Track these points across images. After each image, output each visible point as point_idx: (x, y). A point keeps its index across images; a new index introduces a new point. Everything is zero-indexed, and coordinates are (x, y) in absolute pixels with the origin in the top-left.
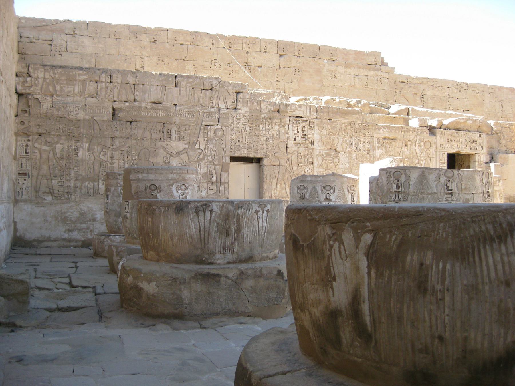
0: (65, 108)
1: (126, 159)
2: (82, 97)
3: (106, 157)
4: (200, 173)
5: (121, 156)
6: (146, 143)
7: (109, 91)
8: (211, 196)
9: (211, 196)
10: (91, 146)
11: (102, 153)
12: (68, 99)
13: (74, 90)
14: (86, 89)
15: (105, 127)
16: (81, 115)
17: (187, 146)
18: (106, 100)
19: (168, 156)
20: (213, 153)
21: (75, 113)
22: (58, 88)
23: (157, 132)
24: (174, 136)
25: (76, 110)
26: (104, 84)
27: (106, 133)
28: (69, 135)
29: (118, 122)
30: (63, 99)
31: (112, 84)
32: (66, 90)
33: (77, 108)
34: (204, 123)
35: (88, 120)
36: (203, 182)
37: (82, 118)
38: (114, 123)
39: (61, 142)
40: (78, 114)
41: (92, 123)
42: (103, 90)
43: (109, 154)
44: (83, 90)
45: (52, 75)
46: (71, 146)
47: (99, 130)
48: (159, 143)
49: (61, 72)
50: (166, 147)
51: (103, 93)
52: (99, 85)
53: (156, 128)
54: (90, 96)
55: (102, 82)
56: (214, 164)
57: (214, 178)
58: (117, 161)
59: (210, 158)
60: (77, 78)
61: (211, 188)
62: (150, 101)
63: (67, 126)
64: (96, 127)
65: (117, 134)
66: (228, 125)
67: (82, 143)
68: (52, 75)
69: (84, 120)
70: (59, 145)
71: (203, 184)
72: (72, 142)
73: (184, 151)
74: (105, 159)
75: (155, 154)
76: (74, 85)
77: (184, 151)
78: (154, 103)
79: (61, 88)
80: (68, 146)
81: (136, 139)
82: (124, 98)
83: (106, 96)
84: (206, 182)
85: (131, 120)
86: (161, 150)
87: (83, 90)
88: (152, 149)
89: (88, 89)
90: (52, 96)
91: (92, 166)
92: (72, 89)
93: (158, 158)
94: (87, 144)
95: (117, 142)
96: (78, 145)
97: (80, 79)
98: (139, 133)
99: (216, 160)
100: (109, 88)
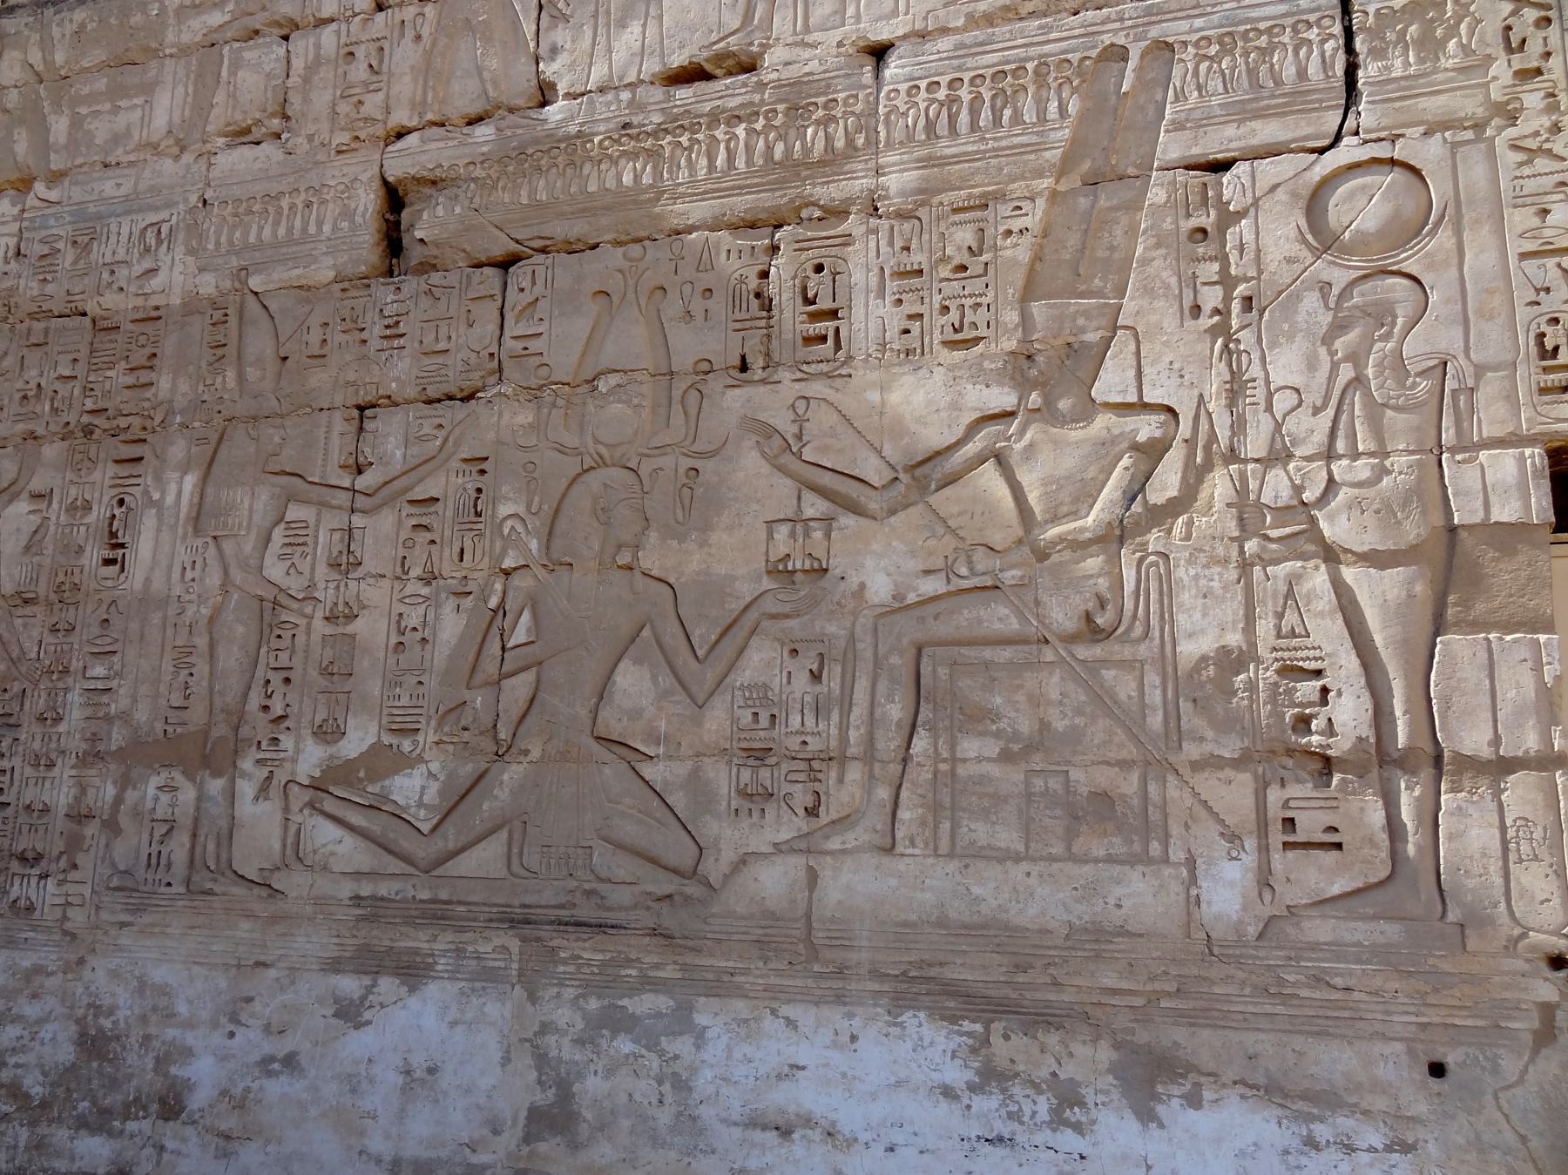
0: (87, 248)
1: (447, 566)
2: (187, 158)
3: (305, 566)
4: (1166, 660)
5: (409, 544)
6: (617, 417)
7: (359, 71)
8: (1320, 929)
9: (1320, 929)
10: (210, 491)
11: (278, 535)
12: (108, 188)
13: (145, 121)
14: (220, 97)
15: (315, 337)
16: (177, 277)
17: (1002, 398)
18: (345, 137)
19: (814, 506)
20: (1310, 429)
21: (138, 269)
22: (59, 127)
23: (718, 305)
24: (871, 317)
25: (147, 250)
26: (328, 33)
27: (319, 378)
28: (88, 431)
29: (411, 284)
30: (77, 194)
31: (380, 17)
32: (101, 130)
33: (151, 238)
34: (1170, 147)
35: (214, 305)
36: (1212, 763)
37: (176, 301)
38: (384, 293)
39: (37, 484)
40: (152, 272)
41: (222, 317)
42: (326, 73)
43: (326, 541)
44: (202, 108)
45: (35, 57)
46: (87, 507)
47: (272, 366)
48: (735, 401)
49: (83, 25)
50: (790, 430)
51: (322, 99)
52: (301, 45)
53: (708, 280)
54: (242, 135)
55: (323, 22)
56: (1331, 555)
57: (1349, 714)
58: (377, 594)
59: (1276, 487)
60: (170, 37)
61: (1310, 825)
62: (652, 66)
63: (80, 370)
64: (260, 343)
65: (400, 373)
66: (1470, 106)
67: (159, 479)
68: (35, 57)
69: (191, 307)
70: (22, 506)
71: (1209, 785)
72: (96, 476)
73: (971, 448)
74: (295, 585)
75: (695, 502)
76: (148, 89)
77: (971, 448)
78: (693, 74)
79: (76, 122)
80: (72, 509)
81: (534, 393)
82: (464, 100)
83: (344, 108)
84: (1238, 763)
85: (500, 246)
86: (750, 464)
87: (202, 108)
88: (667, 462)
89: (233, 96)
90: (24, 185)
91: (201, 642)
92: (138, 113)
93: (719, 537)
94: (190, 481)
95: (391, 440)
96: (135, 496)
97: (186, 38)
98: (563, 340)
99: (1356, 505)
100: (361, 52)
